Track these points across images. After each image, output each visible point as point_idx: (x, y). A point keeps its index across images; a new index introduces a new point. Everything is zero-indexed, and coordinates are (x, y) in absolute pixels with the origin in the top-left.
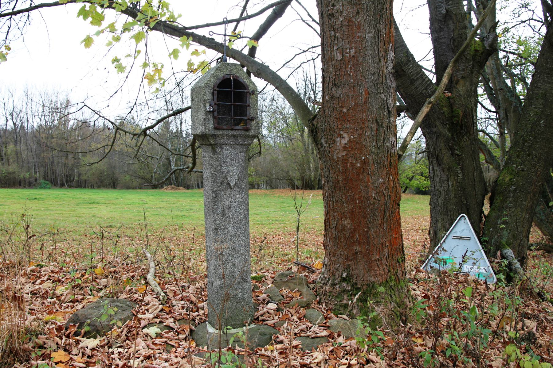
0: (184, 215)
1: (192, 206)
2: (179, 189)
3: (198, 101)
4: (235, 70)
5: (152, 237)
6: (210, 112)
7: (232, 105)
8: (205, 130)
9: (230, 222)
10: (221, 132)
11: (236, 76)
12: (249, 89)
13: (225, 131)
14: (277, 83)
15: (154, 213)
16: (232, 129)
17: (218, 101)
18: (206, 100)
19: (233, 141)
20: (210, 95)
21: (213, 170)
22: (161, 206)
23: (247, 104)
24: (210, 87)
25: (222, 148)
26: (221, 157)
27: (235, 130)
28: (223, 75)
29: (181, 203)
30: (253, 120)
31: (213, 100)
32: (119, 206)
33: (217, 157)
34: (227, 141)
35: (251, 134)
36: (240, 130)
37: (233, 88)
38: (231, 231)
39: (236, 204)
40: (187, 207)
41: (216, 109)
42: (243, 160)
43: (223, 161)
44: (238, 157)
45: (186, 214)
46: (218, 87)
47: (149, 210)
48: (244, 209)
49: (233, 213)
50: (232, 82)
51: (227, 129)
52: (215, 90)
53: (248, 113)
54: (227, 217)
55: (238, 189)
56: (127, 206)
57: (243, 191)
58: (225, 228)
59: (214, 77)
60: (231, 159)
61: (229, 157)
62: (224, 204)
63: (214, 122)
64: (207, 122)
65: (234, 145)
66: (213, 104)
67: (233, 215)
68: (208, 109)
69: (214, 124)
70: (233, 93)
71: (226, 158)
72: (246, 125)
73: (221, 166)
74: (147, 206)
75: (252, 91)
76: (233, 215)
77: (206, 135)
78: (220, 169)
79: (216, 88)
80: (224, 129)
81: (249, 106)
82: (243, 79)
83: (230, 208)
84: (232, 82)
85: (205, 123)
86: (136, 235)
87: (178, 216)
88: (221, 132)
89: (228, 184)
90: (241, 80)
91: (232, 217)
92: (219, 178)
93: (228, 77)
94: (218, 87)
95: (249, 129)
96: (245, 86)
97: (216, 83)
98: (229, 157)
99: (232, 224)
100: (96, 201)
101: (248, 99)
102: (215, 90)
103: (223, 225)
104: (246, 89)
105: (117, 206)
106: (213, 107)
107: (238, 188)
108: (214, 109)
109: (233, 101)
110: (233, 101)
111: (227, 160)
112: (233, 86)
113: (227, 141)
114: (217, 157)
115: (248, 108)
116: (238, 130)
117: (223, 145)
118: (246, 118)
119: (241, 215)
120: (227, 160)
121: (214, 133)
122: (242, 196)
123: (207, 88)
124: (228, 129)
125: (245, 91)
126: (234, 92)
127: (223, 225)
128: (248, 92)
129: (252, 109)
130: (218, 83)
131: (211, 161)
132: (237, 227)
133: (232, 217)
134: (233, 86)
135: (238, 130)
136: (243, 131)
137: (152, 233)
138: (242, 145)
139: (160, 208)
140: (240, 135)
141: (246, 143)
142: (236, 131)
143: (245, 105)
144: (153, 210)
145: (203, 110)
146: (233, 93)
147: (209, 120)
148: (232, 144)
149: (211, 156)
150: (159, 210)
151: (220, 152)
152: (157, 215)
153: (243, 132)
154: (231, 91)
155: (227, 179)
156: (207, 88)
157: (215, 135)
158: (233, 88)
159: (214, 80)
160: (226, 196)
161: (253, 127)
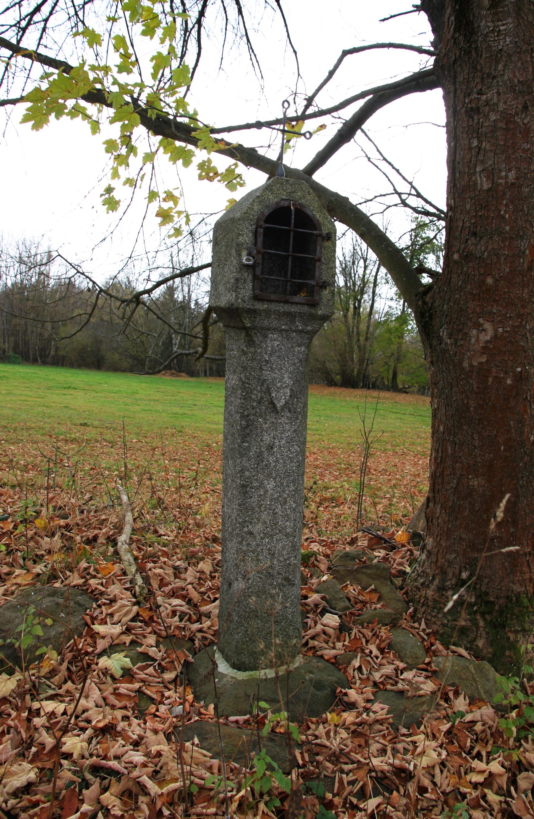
0: (185, 414)
1: (196, 401)
2: (181, 376)
3: (227, 246)
4: (299, 194)
6: (248, 266)
7: (289, 255)
8: (236, 301)
9: (269, 475)
10: (266, 306)
11: (301, 205)
12: (321, 230)
14: (363, 226)
15: (146, 408)
16: (286, 302)
17: (264, 248)
18: (242, 244)
19: (286, 324)
20: (251, 235)
21: (245, 376)
22: (156, 398)
23: (316, 257)
24: (251, 220)
25: (265, 336)
26: (261, 353)
28: (276, 200)
29: (182, 395)
30: (326, 288)
31: (256, 244)
32: (102, 395)
33: (255, 352)
34: (275, 324)
35: (320, 312)
37: (292, 225)
38: (270, 492)
39: (284, 442)
40: (190, 402)
41: (260, 261)
42: (301, 361)
43: (266, 360)
44: (294, 355)
45: (187, 412)
47: (139, 402)
48: (296, 451)
49: (277, 458)
50: (293, 213)
51: (276, 301)
52: (261, 227)
53: (317, 274)
54: (266, 465)
55: (288, 415)
56: (112, 395)
58: (261, 485)
59: (260, 202)
60: (279, 357)
61: (277, 354)
62: (262, 441)
63: (253, 286)
65: (287, 331)
66: (255, 252)
67: (277, 461)
68: (244, 261)
69: (253, 290)
71: (271, 355)
72: (313, 296)
73: (261, 369)
74: (137, 396)
75: (327, 234)
76: (277, 461)
77: (237, 309)
78: (259, 376)
79: (262, 223)
80: (271, 301)
81: (320, 260)
82: (312, 211)
83: (272, 448)
84: (293, 213)
85: (237, 287)
87: (176, 414)
88: (266, 306)
89: (272, 403)
90: (309, 213)
91: (275, 466)
92: (255, 392)
93: (286, 204)
94: (266, 221)
95: (318, 304)
97: (262, 213)
98: (277, 354)
99: (274, 479)
100: (73, 386)
101: (318, 248)
102: (261, 227)
103: (256, 480)
104: (316, 229)
105: (98, 395)
106: (254, 258)
107: (290, 411)
108: (255, 262)
109: (291, 249)
110: (291, 249)
111: (273, 359)
112: (293, 221)
113: (275, 324)
114: (255, 352)
115: (318, 264)
116: (297, 304)
117: (268, 329)
118: (313, 283)
119: (292, 462)
120: (273, 359)
121: (252, 307)
122: (296, 428)
123: (246, 222)
125: (315, 232)
126: (294, 231)
127: (256, 480)
128: (320, 235)
129: (324, 267)
130: (267, 212)
131: (243, 358)
132: (282, 484)
133: (275, 466)
134: (293, 221)
135: (297, 304)
137: (140, 438)
138: (301, 331)
139: (154, 400)
140: (300, 313)
141: (309, 328)
142: (294, 306)
144: (144, 402)
145: (235, 262)
147: (245, 281)
148: (283, 330)
149: (243, 350)
150: (152, 403)
151: (261, 342)
152: (149, 410)
153: (306, 309)
154: (289, 231)
155: (270, 395)
156: (246, 222)
157: (255, 311)
158: (292, 225)
159: (260, 207)
160: (267, 426)
161: (324, 300)
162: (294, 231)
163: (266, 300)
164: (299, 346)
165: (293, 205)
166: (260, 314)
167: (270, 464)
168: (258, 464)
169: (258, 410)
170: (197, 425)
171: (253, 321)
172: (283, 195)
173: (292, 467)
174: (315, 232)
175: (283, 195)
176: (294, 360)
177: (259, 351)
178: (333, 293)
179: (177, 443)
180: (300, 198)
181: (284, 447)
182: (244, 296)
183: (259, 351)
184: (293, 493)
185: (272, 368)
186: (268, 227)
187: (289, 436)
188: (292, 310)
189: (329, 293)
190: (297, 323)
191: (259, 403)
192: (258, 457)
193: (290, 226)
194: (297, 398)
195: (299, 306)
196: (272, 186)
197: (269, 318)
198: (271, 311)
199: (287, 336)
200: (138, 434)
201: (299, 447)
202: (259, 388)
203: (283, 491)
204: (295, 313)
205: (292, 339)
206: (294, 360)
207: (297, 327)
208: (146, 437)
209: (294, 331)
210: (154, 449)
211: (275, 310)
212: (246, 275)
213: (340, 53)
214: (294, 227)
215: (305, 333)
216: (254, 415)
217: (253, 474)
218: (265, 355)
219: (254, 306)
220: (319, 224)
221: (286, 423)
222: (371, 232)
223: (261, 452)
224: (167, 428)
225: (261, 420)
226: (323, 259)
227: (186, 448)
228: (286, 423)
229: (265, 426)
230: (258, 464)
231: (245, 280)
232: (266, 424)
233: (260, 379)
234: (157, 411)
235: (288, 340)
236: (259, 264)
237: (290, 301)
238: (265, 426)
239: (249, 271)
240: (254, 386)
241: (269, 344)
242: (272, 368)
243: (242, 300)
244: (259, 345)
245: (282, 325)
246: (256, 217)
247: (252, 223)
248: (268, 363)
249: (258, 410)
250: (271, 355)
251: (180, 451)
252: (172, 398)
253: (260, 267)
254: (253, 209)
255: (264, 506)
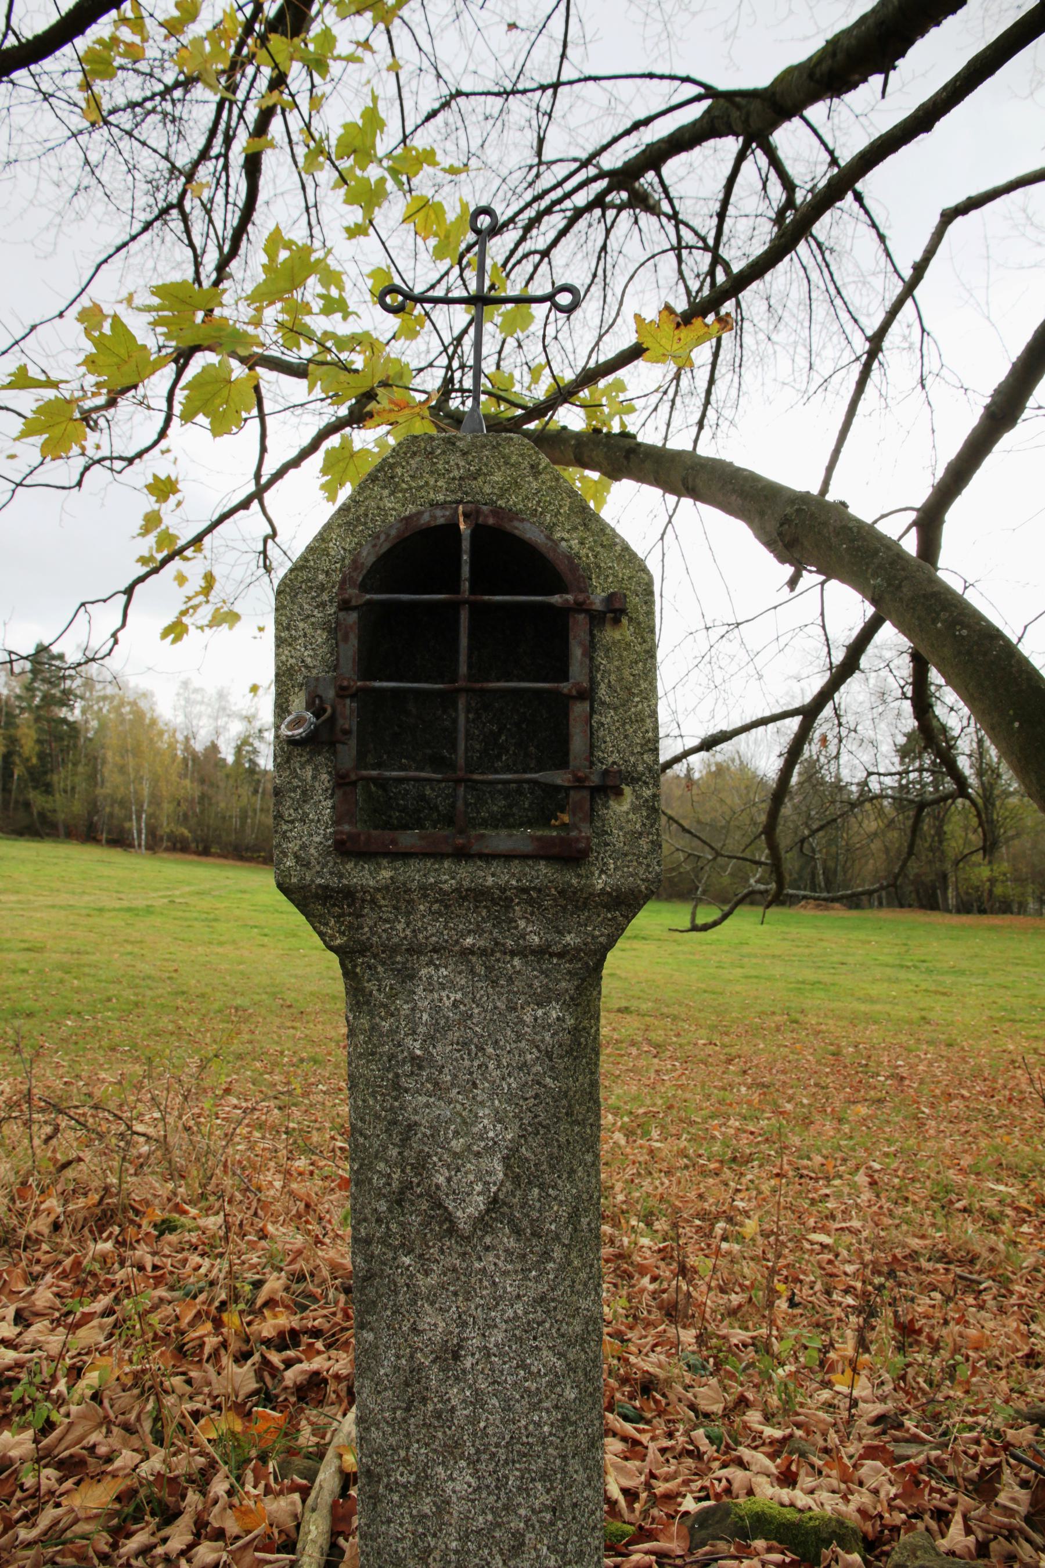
0: (819, 982)
1: (848, 955)
2: (833, 909)
4: (497, 477)
5: (709, 1050)
7: (458, 691)
9: (453, 1448)
10: (386, 874)
11: (497, 512)
13: (415, 864)
14: (875, 575)
15: (753, 973)
16: (462, 855)
19: (478, 931)
22: (777, 952)
24: (322, 588)
25: (408, 975)
27: (488, 858)
29: (825, 944)
33: (374, 1028)
34: (434, 930)
35: (600, 883)
36: (524, 857)
38: (457, 1508)
39: (498, 1336)
40: (835, 959)
42: (549, 1055)
43: (414, 1058)
44: (519, 1037)
46: (364, 587)
47: (746, 960)
48: (552, 1370)
49: (477, 1392)
50: (466, 545)
53: (578, 744)
54: (437, 1414)
55: (511, 1243)
57: (546, 1256)
58: (423, 1483)
62: (414, 1329)
64: (289, 813)
65: (484, 952)
67: (478, 1400)
70: (464, 616)
71: (430, 1039)
74: (745, 950)
75: (611, 598)
76: (478, 1400)
79: (353, 592)
80: (405, 856)
81: (587, 694)
82: (551, 528)
83: (456, 1357)
84: (466, 545)
86: (674, 1039)
87: (803, 982)
88: (386, 874)
91: (474, 1420)
92: (381, 1166)
93: (441, 517)
94: (364, 587)
96: (563, 567)
98: (455, 1035)
99: (473, 1463)
103: (406, 1461)
104: (561, 588)
105: (680, 948)
107: (517, 1232)
109: (463, 669)
110: (463, 669)
111: (438, 1051)
112: (465, 571)
113: (434, 930)
114: (374, 1028)
115: (580, 709)
116: (508, 857)
119: (535, 1407)
120: (438, 1051)
121: (334, 882)
122: (543, 1288)
124: (438, 856)
125: (556, 599)
126: (474, 607)
127: (406, 1461)
128: (580, 607)
129: (608, 717)
130: (368, 556)
132: (501, 1483)
133: (474, 1420)
134: (465, 571)
136: (543, 868)
138: (541, 952)
139: (774, 956)
140: (525, 890)
142: (495, 866)
143: (556, 694)
144: (754, 961)
146: (464, 616)
147: (306, 796)
151: (393, 996)
152: (756, 977)
153: (543, 872)
154: (454, 607)
156: (300, 599)
157: (348, 894)
159: (350, 543)
160: (432, 1280)
161: (618, 839)
162: (474, 607)
163: (386, 854)
164: (540, 1005)
165: (466, 515)
166: (373, 901)
167: (453, 1409)
168: (407, 1410)
169: (394, 1227)
170: (834, 1005)
171: (350, 927)
172: (436, 489)
173: (538, 1425)
174: (556, 599)
175: (436, 489)
176: (522, 1053)
177: (385, 1025)
178: (652, 809)
179: (779, 1046)
180: (503, 492)
181: (501, 1355)
182: (303, 847)
183: (385, 1025)
184: (548, 1516)
185: (436, 1084)
186: (369, 602)
187: (516, 1317)
188: (490, 881)
189: (635, 809)
190: (522, 924)
191: (399, 1202)
192: (407, 1384)
193: (456, 590)
194: (542, 1187)
195: (516, 866)
196: (392, 466)
197: (408, 914)
198: (408, 891)
199: (489, 969)
200: (713, 1028)
201: (561, 1355)
202: (394, 1152)
203: (506, 1508)
204: (503, 890)
205: (510, 980)
206: (522, 1053)
207: (523, 936)
208: (727, 1034)
209: (513, 954)
210: (729, 1061)
211: (423, 888)
212: (309, 773)
213: (936, 220)
214: (473, 591)
215: (560, 955)
216: (383, 1241)
217: (393, 1441)
218: (408, 1041)
219: (341, 876)
220: (574, 568)
221: (505, 1273)
222: (899, 587)
223: (417, 1371)
224: (773, 1013)
225: (407, 1260)
226: (602, 691)
227: (791, 1057)
228: (505, 1273)
229: (424, 1283)
230: (407, 1410)
231: (304, 793)
232: (427, 1274)
233: (395, 1122)
234: (770, 979)
235: (494, 983)
236: (347, 732)
237: (475, 848)
238: (424, 1283)
239: (320, 759)
240: (376, 1144)
241: (423, 999)
242: (436, 1084)
243: (296, 857)
244: (384, 1006)
245: (463, 936)
246: (337, 577)
247: (325, 597)
248: (421, 1068)
249: (394, 1227)
250: (430, 1039)
251: (779, 1065)
252: (807, 951)
253: (353, 742)
254: (326, 552)
255: (437, 1554)
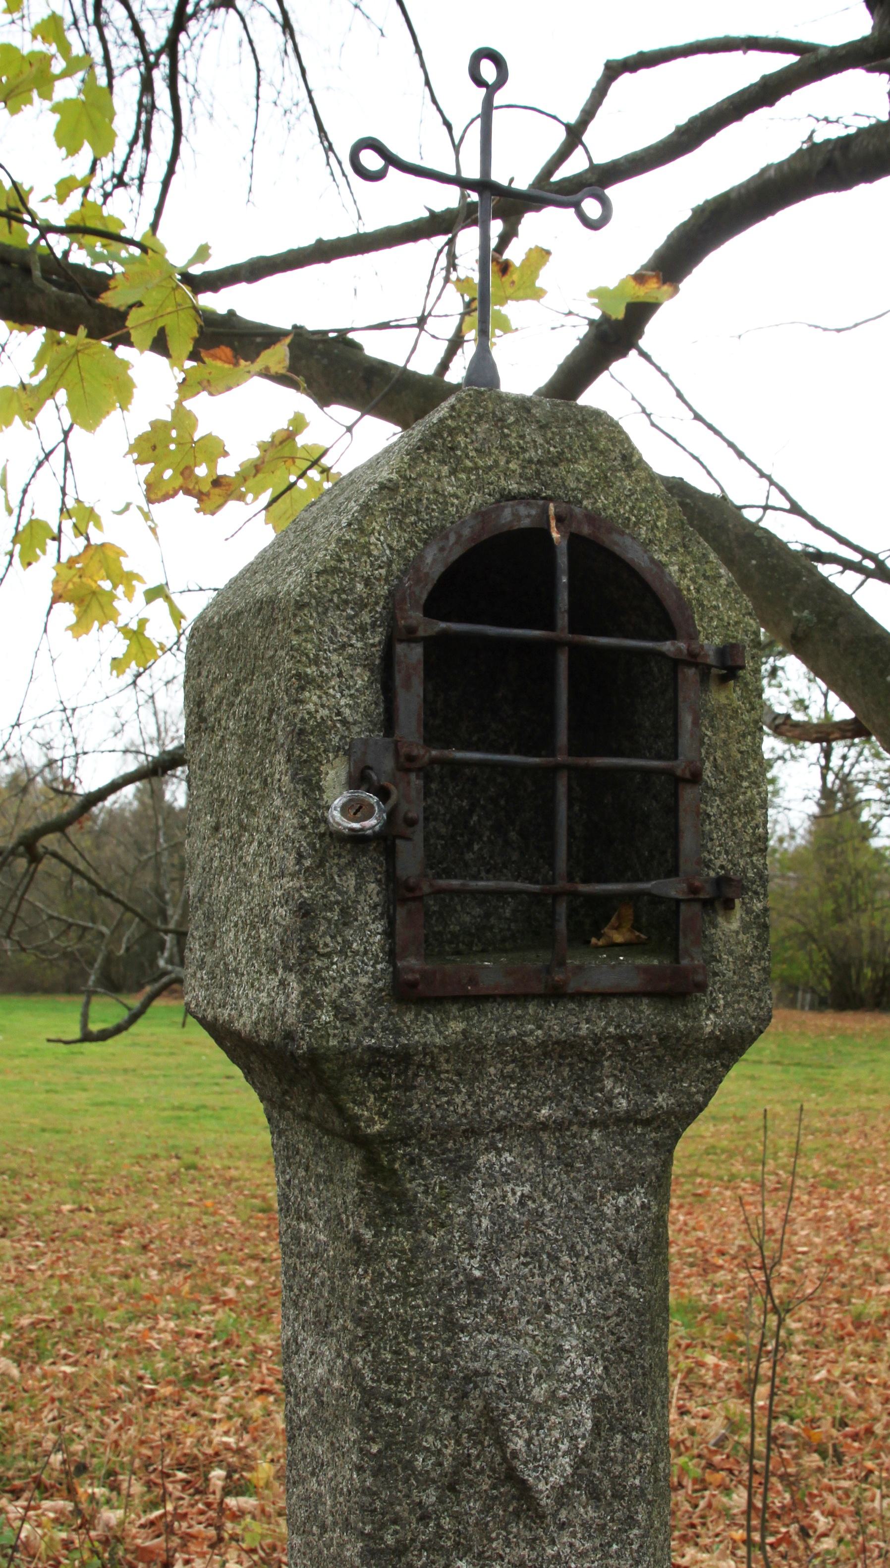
0: (204, 1107)
3: (247, 739)
5: (82, 1218)
6: (357, 839)
8: (308, 1017)
10: (456, 1026)
11: (592, 518)
12: (693, 636)
13: (494, 1010)
14: (800, 606)
15: (103, 1098)
17: (431, 738)
18: (322, 730)
19: (557, 1097)
20: (361, 678)
21: (377, 1363)
22: (129, 1064)
23: (680, 766)
24: (361, 604)
26: (444, 1249)
27: (582, 997)
28: (476, 499)
30: (729, 905)
31: (389, 723)
33: (419, 1247)
35: (709, 1024)
36: (623, 995)
37: (563, 620)
41: (416, 811)
42: (632, 1255)
43: (472, 1282)
45: (211, 1100)
46: (432, 608)
47: (86, 1079)
50: (563, 561)
51: (507, 997)
52: (410, 635)
53: (687, 842)
56: (17, 1062)
57: (630, 1521)
59: (400, 513)
60: (533, 1254)
61: (523, 1243)
63: (389, 934)
64: (326, 943)
65: (560, 1126)
66: (388, 764)
68: (335, 815)
69: (392, 955)
70: (563, 660)
72: (674, 951)
73: (451, 1326)
77: (314, 1057)
78: (444, 1360)
79: (416, 616)
80: (479, 1000)
81: (696, 778)
84: (563, 561)
85: (309, 948)
86: (24, 1207)
87: (180, 1108)
88: (456, 1026)
89: (512, 1477)
90: (634, 555)
92: (429, 1441)
94: (432, 608)
95: (701, 987)
96: (670, 603)
97: (413, 567)
98: (523, 1243)
101: (687, 720)
102: (410, 635)
104: (669, 631)
106: (383, 794)
107: (595, 1495)
108: (391, 814)
109: (562, 738)
110: (562, 738)
112: (563, 599)
115: (688, 794)
116: (605, 996)
117: (473, 1132)
118: (673, 888)
121: (388, 1042)
123: (332, 617)
124: (520, 998)
125: (667, 647)
128: (693, 659)
131: (361, 1278)
134: (563, 599)
135: (605, 996)
136: (646, 1008)
137: (83, 1197)
138: (630, 1119)
139: (126, 1071)
140: (621, 1039)
141: (662, 1100)
142: (591, 1009)
143: (669, 773)
145: (289, 819)
146: (563, 660)
147: (347, 916)
148: (544, 1126)
149: (357, 1239)
150: (119, 1079)
152: (111, 1103)
154: (549, 648)
155: (500, 1443)
156: (332, 617)
157: (404, 1057)
158: (563, 620)
159: (398, 537)
161: (727, 966)
163: (455, 999)
164: (620, 1190)
165: (560, 519)
169: (446, 1522)
170: (236, 1139)
172: (507, 474)
174: (667, 647)
175: (507, 474)
177: (434, 1241)
179: (181, 1205)
182: (346, 992)
183: (434, 1241)
186: (444, 635)
190: (608, 1084)
191: (452, 1488)
193: (549, 624)
195: (614, 1008)
196: (452, 431)
200: (76, 1186)
202: (446, 1418)
204: (597, 1040)
205: (588, 1161)
206: (603, 1256)
208: (99, 1192)
209: (593, 1124)
210: (118, 1232)
211: (501, 1042)
212: (350, 881)
213: (598, 72)
214: (573, 628)
215: (646, 1123)
218: (464, 1259)
219: (398, 1032)
220: (684, 605)
222: (834, 625)
224: (156, 1157)
227: (206, 1220)
231: (344, 912)
233: (446, 1376)
234: (131, 1105)
235: (569, 1166)
237: (572, 987)
239: (364, 861)
240: (422, 1411)
243: (337, 1008)
244: (431, 1213)
245: (539, 1105)
246: (382, 590)
247: (366, 617)
248: (480, 1294)
249: (446, 1522)
250: (492, 1253)
251: (192, 1233)
252: (171, 1061)
253: (418, 835)
